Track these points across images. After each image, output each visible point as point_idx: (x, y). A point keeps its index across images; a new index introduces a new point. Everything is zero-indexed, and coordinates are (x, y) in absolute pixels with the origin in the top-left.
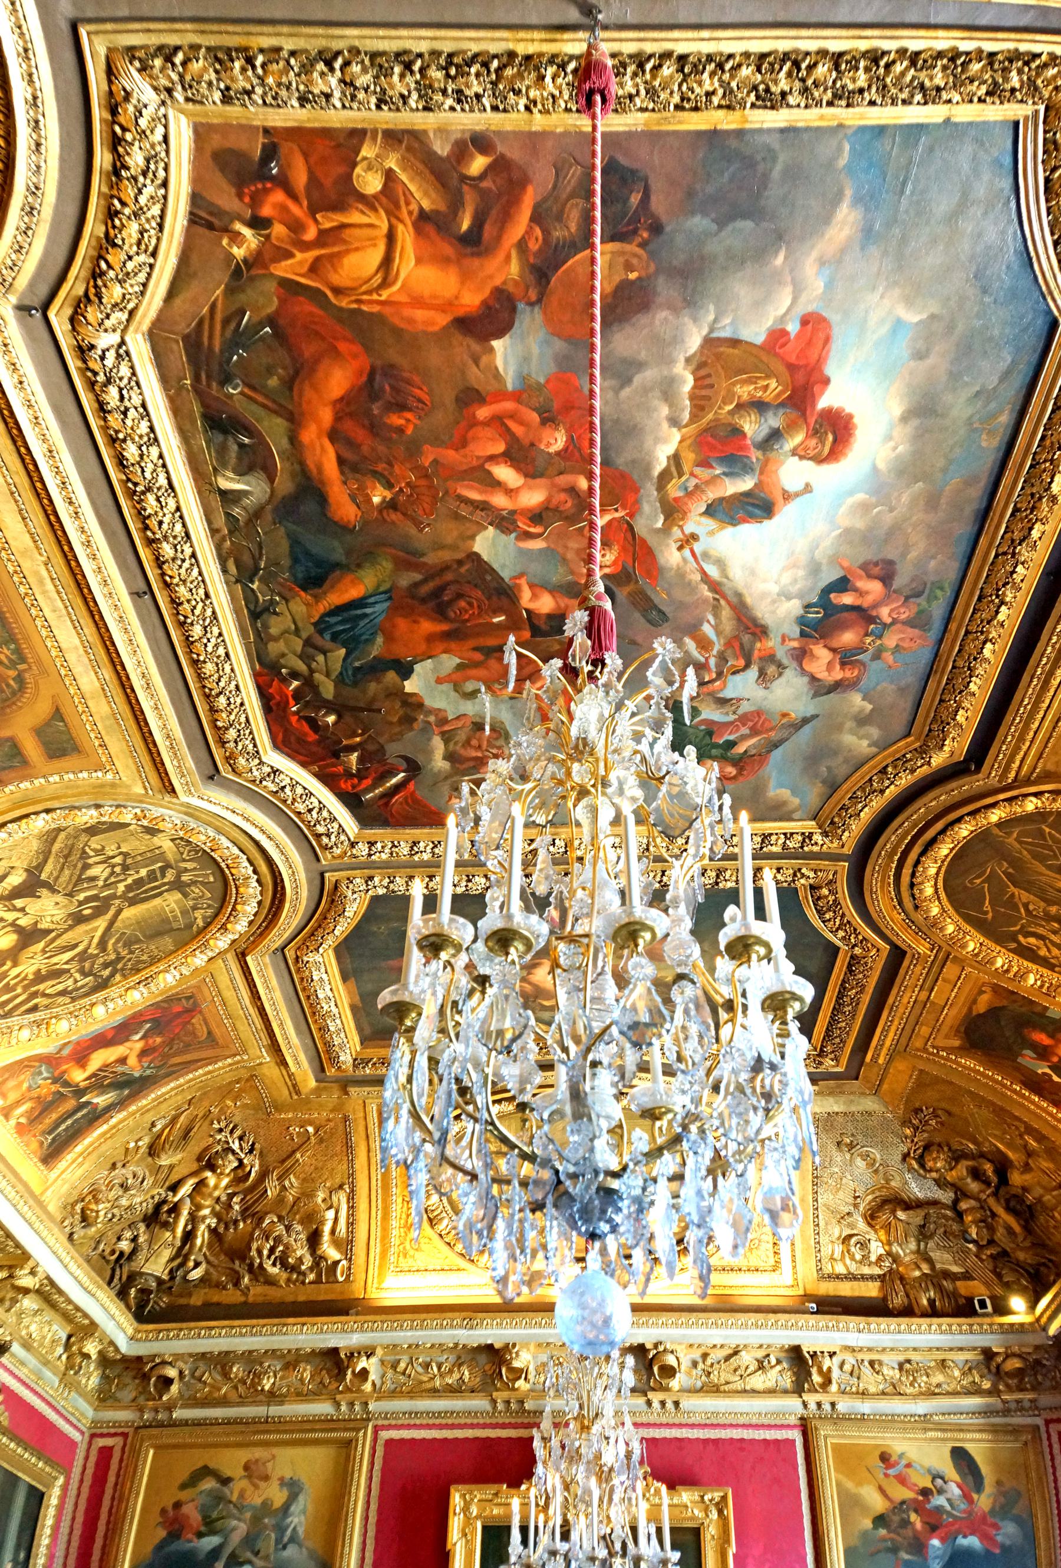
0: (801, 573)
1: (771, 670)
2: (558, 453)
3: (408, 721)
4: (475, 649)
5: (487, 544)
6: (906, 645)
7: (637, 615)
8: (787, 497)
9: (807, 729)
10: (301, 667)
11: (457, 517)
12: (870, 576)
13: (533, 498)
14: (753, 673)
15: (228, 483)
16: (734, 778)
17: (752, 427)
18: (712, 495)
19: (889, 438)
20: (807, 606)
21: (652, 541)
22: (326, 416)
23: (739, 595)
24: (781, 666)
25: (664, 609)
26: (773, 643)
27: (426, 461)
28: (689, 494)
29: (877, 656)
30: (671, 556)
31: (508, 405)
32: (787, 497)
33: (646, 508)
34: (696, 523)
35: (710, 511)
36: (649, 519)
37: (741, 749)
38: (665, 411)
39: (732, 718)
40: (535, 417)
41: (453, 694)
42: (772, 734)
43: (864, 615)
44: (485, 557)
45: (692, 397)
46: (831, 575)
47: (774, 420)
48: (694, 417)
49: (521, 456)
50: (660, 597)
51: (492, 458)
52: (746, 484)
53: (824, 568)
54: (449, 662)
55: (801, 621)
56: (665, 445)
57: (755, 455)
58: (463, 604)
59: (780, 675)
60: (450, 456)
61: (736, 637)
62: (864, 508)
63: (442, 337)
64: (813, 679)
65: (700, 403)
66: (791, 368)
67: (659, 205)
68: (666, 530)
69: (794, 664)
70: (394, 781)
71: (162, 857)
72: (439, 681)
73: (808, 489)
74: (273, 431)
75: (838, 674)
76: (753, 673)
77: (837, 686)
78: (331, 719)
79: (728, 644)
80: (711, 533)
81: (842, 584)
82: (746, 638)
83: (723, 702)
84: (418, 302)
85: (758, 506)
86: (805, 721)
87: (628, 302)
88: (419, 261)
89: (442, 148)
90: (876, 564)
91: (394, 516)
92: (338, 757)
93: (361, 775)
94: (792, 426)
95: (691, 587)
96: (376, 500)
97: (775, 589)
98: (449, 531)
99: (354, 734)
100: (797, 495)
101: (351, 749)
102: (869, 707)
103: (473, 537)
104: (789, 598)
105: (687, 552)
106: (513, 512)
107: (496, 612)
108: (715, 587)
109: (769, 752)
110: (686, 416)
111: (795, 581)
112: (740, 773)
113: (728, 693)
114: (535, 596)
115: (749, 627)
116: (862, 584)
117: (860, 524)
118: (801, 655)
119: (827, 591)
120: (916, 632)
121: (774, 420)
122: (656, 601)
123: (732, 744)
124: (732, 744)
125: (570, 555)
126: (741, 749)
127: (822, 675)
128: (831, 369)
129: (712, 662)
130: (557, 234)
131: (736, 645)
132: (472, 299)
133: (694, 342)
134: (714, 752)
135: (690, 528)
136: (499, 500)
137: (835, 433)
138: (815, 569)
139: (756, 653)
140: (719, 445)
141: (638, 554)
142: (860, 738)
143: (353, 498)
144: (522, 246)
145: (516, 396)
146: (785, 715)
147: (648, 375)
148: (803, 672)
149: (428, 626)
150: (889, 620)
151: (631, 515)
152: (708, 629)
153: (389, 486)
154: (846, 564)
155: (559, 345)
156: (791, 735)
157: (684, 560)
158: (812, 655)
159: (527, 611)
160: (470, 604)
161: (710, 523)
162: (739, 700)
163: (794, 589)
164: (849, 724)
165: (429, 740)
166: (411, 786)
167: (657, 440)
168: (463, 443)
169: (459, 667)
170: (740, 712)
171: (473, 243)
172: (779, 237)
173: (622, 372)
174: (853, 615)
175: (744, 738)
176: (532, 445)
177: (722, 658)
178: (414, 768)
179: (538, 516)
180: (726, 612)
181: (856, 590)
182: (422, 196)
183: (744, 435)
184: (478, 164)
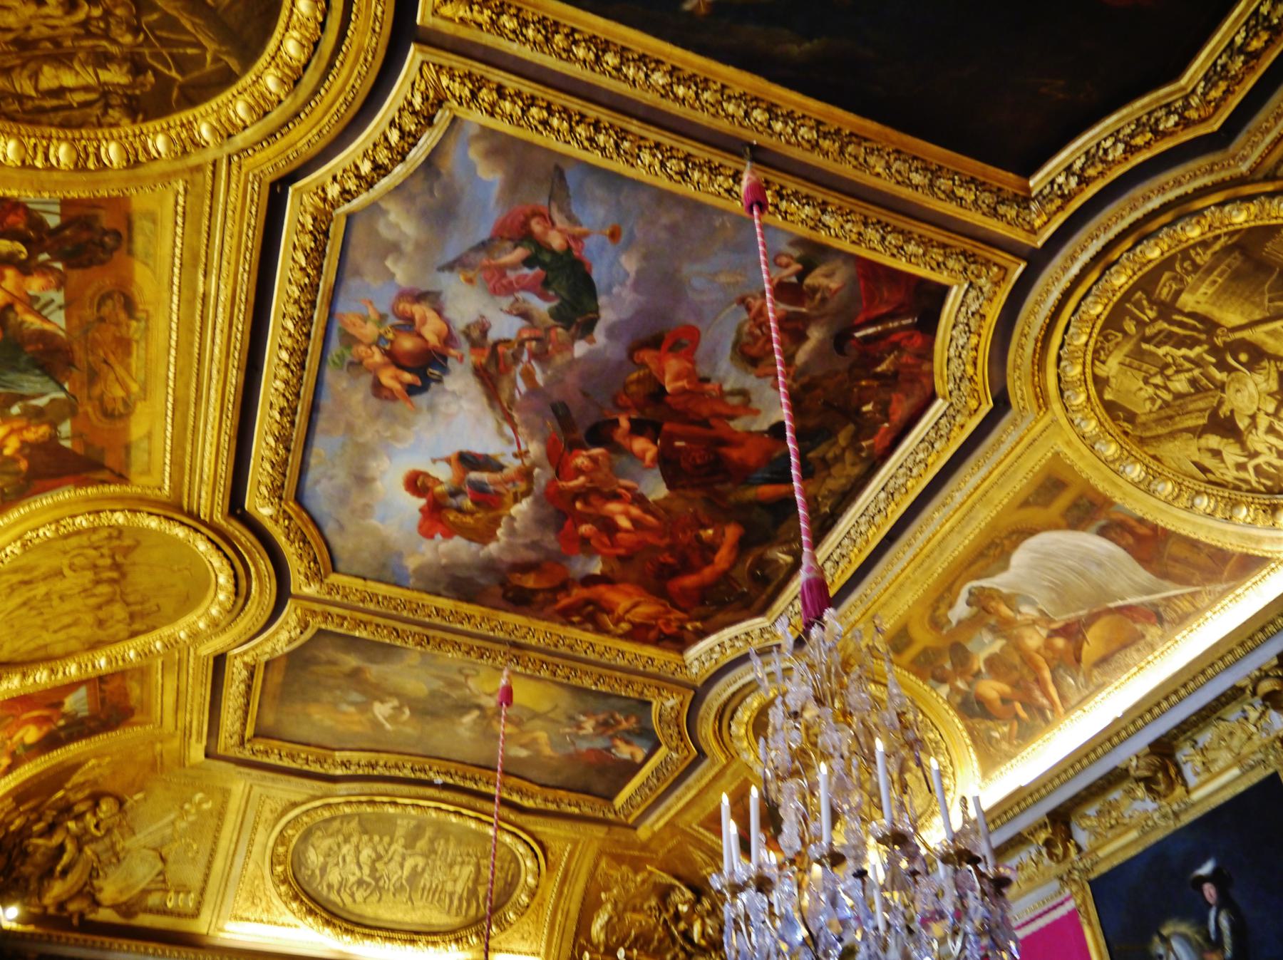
0: (442, 408)
1: (475, 334)
2: (586, 522)
3: (806, 388)
4: (710, 427)
5: (657, 490)
6: (359, 322)
7: (574, 416)
8: (448, 460)
9: (451, 256)
10: (849, 456)
11: (667, 511)
12: (391, 390)
13: (614, 507)
14: (493, 335)
15: (789, 559)
16: (536, 214)
17: (467, 503)
18: (498, 476)
19: (383, 473)
20: (439, 381)
21: (546, 463)
22: (707, 572)
23: (492, 406)
24: (467, 334)
25: (551, 414)
26: (470, 359)
27: (667, 541)
28: (513, 481)
29: (382, 318)
30: (535, 449)
31: (605, 550)
32: (448, 460)
33: (543, 482)
34: (513, 464)
35: (501, 468)
36: (542, 476)
37: (520, 253)
38: (516, 525)
39: (521, 295)
40: (593, 542)
41: (754, 397)
42: (485, 262)
43: (394, 359)
44: (664, 485)
45: (499, 525)
46: (421, 400)
47: (453, 502)
48: (500, 517)
49: (608, 526)
50: (551, 424)
51: (627, 531)
52: (474, 475)
53: (425, 408)
54: (738, 425)
55: (445, 370)
56: (521, 509)
57: (467, 489)
58: (699, 461)
59: (468, 327)
60: (650, 539)
61: (500, 373)
62: (396, 438)
63: (624, 580)
64: (439, 312)
65: (496, 522)
66: (441, 521)
67: (499, 591)
68: (534, 465)
69: (455, 333)
70: (870, 331)
71: (1138, 354)
72: (757, 412)
73: (434, 461)
74: (741, 572)
75: (418, 310)
76: (493, 335)
77: (420, 297)
78: (867, 408)
79: (507, 370)
80: (503, 455)
81: (411, 390)
82: (492, 370)
83: (525, 315)
84: (628, 595)
85: (467, 461)
86: (450, 267)
87: (525, 568)
88: (618, 604)
89: (590, 626)
90: (386, 398)
91: (705, 520)
92: (896, 374)
93: (896, 346)
94: (442, 495)
95: (527, 423)
96: (710, 532)
97: (465, 404)
98: (678, 505)
99: (862, 388)
100: (441, 460)
101: (878, 376)
102: (389, 263)
103: (666, 498)
104: (454, 393)
105: (523, 447)
106: (631, 503)
107: (680, 448)
108: (509, 418)
109: (492, 239)
110: (504, 519)
111: (447, 404)
112: (526, 224)
113: (518, 323)
114: (644, 452)
115: (490, 377)
116: (396, 386)
117: (400, 430)
118: (448, 339)
119: (423, 389)
120: (352, 330)
121: (453, 502)
122: (556, 422)
123: (528, 262)
124: (528, 262)
125: (606, 470)
126: (520, 253)
127: (431, 315)
128: (418, 515)
129: (525, 357)
130: (549, 596)
131: (502, 366)
132: (602, 589)
133: (493, 548)
134: (547, 258)
135: (517, 463)
136: (635, 511)
137: (416, 483)
138: (432, 408)
139: (487, 352)
140: (488, 500)
141: (557, 458)
142: (397, 226)
143: (724, 534)
144: (568, 595)
145: (597, 552)
146: (470, 281)
147: (520, 541)
148: (447, 323)
149: (735, 454)
150: (374, 349)
151: (553, 481)
152: (522, 386)
153: (698, 538)
154: (409, 405)
155: (566, 564)
156: (466, 255)
157: (526, 443)
158: (439, 336)
159: (655, 443)
160: (694, 459)
161: (503, 460)
162: (510, 312)
163: (447, 398)
164: (408, 248)
165: (806, 364)
166: (861, 318)
167: (525, 513)
168: (639, 543)
169: (732, 418)
170: (511, 299)
171: (588, 602)
172: (445, 567)
173: (534, 545)
174: (404, 362)
175: (514, 266)
176: (600, 530)
177: (516, 358)
178: (840, 340)
179: (616, 497)
180: (504, 396)
181: (401, 383)
182: (606, 619)
183: (472, 501)
184: (576, 619)
